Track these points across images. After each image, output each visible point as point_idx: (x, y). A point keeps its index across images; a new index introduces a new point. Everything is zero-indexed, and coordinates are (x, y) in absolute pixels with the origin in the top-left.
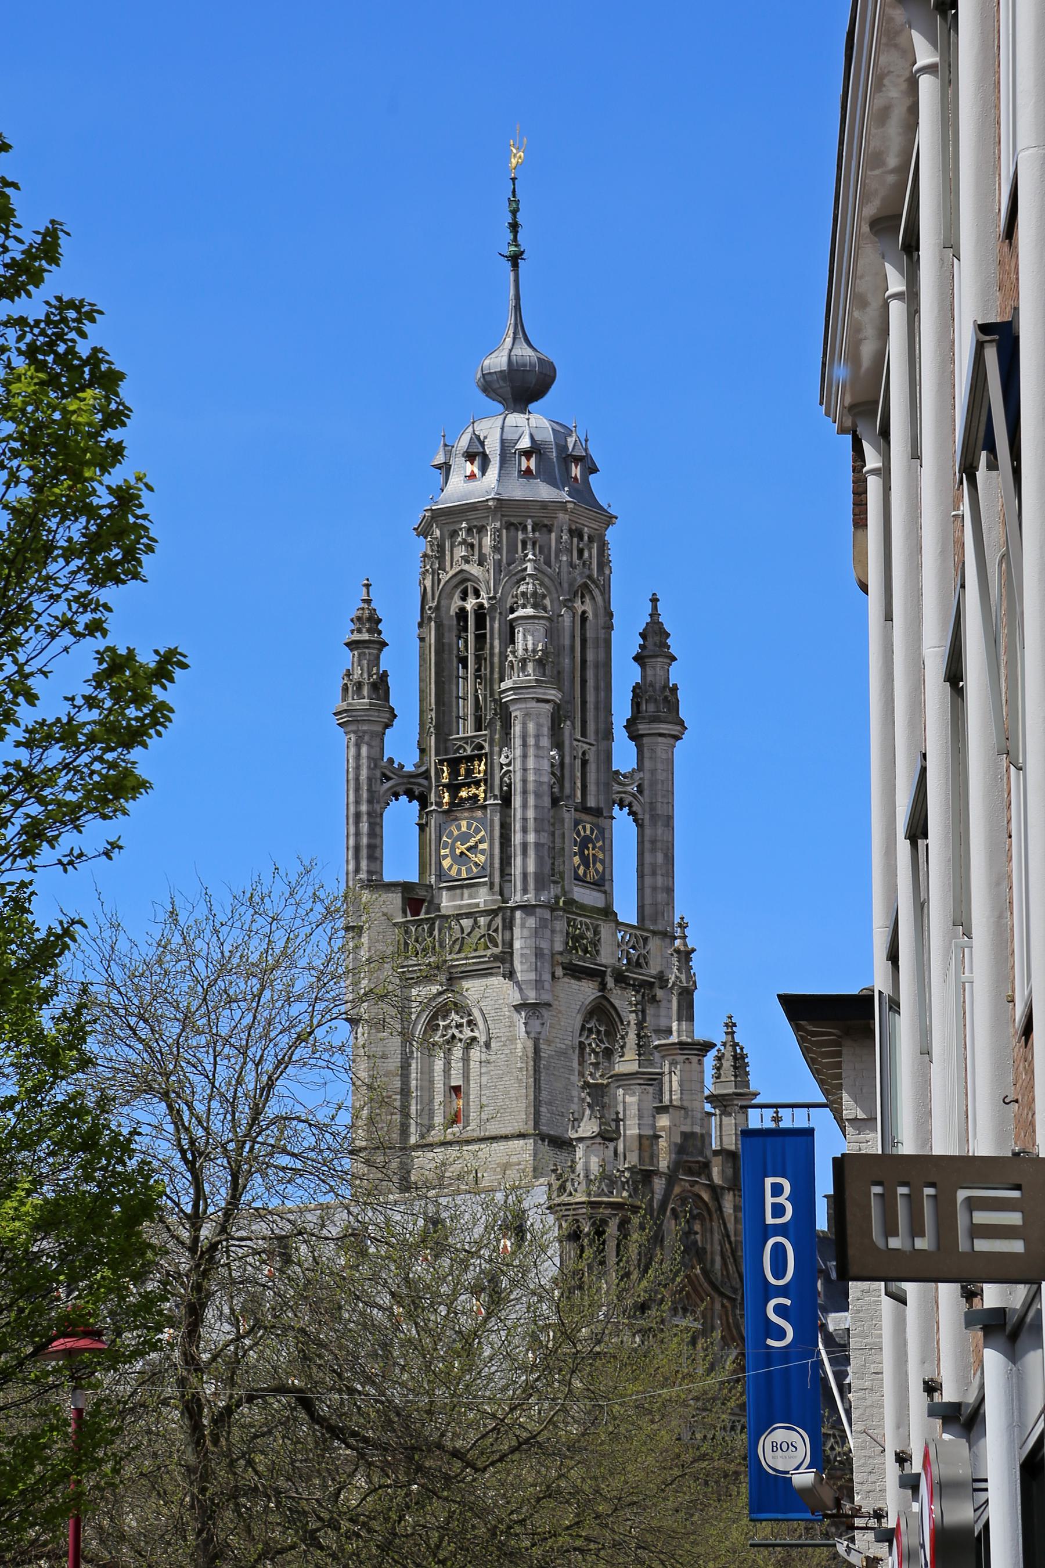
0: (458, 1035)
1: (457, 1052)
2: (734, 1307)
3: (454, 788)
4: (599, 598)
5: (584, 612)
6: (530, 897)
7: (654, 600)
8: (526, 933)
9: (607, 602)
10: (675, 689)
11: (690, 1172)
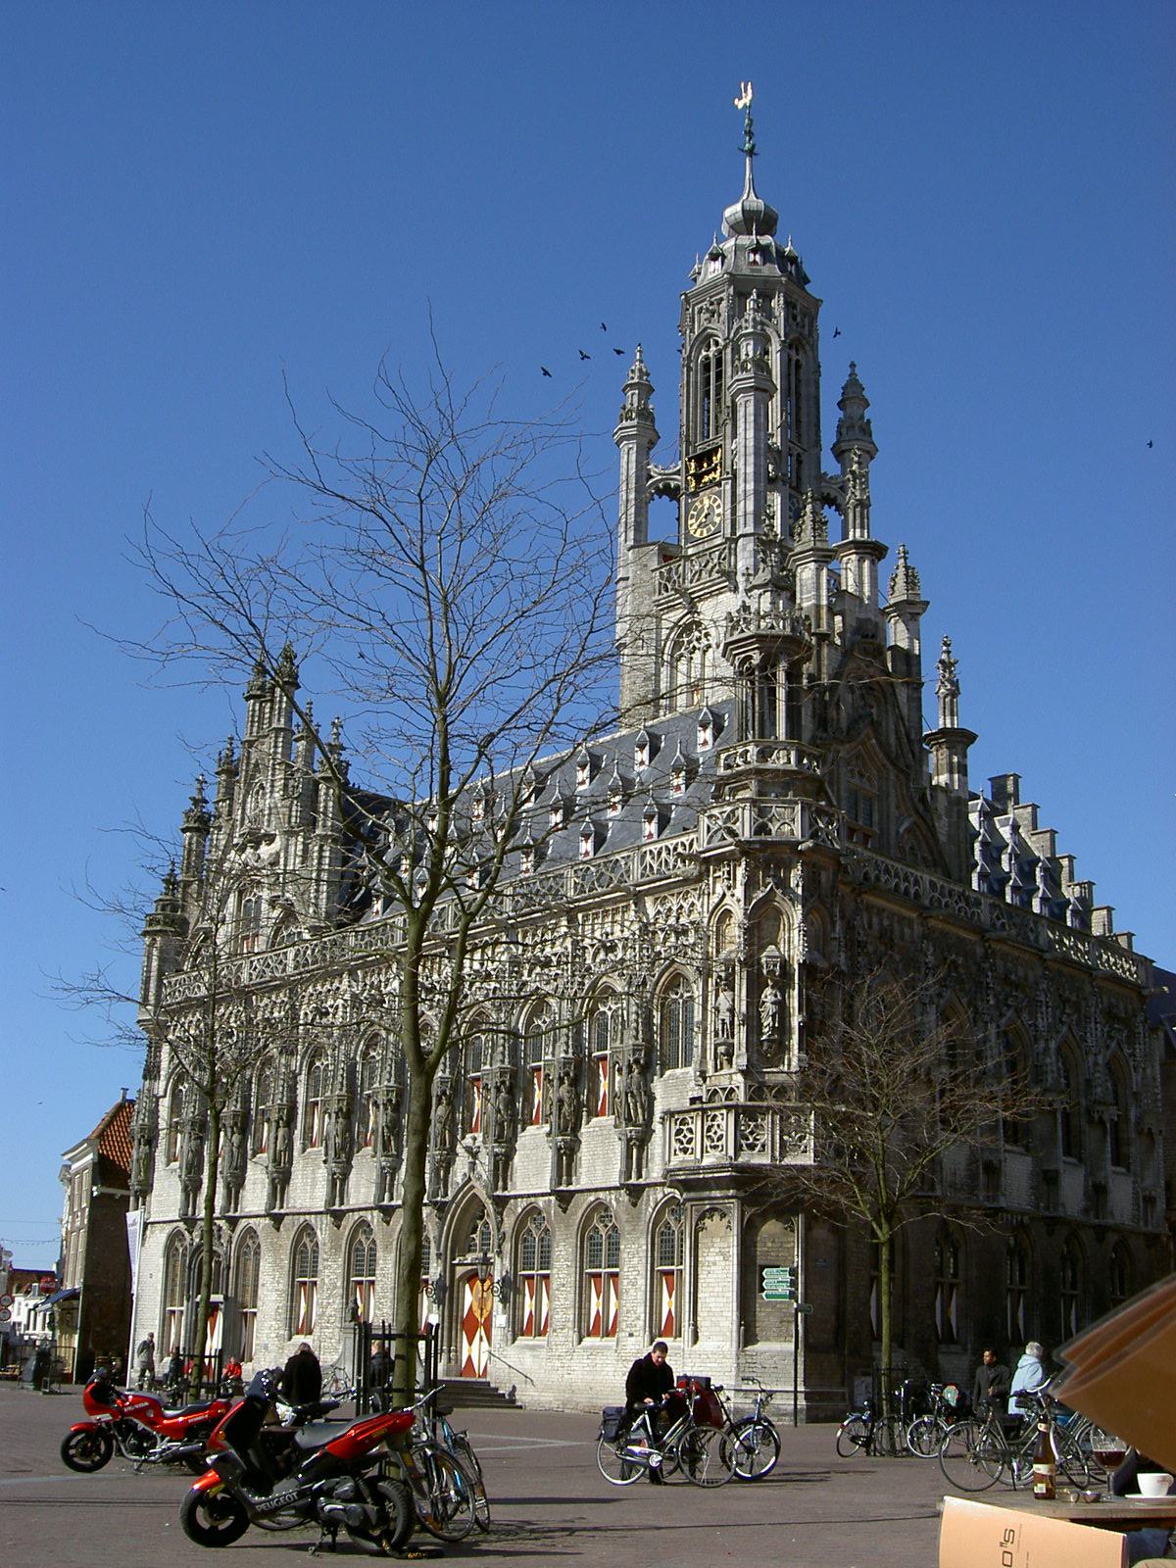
0: (697, 645)
1: (697, 655)
2: (907, 779)
3: (698, 477)
4: (810, 353)
5: (798, 361)
6: (750, 529)
7: (853, 365)
8: (747, 554)
9: (816, 358)
10: (869, 421)
11: (866, 652)
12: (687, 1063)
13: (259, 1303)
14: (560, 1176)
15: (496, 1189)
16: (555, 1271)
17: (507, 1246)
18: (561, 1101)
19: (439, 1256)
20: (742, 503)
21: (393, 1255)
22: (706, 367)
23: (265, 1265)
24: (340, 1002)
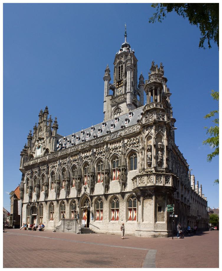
3: (118, 85)
12: (135, 168)
13: (43, 215)
14: (105, 191)
15: (91, 194)
16: (104, 209)
17: (93, 205)
18: (106, 177)
19: (78, 207)
20: (128, 87)
21: (69, 207)
22: (119, 68)
23: (44, 209)
24: (57, 164)
